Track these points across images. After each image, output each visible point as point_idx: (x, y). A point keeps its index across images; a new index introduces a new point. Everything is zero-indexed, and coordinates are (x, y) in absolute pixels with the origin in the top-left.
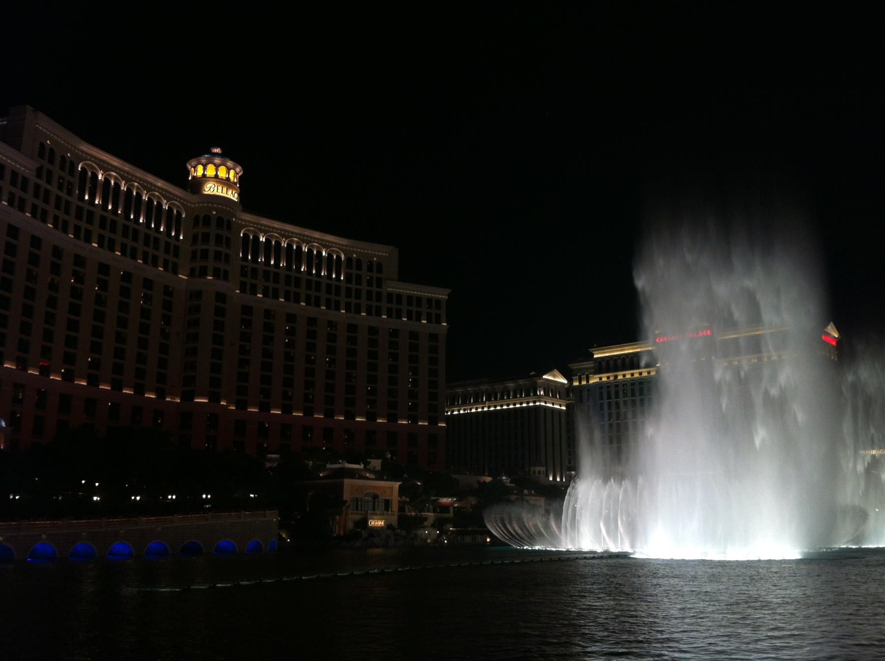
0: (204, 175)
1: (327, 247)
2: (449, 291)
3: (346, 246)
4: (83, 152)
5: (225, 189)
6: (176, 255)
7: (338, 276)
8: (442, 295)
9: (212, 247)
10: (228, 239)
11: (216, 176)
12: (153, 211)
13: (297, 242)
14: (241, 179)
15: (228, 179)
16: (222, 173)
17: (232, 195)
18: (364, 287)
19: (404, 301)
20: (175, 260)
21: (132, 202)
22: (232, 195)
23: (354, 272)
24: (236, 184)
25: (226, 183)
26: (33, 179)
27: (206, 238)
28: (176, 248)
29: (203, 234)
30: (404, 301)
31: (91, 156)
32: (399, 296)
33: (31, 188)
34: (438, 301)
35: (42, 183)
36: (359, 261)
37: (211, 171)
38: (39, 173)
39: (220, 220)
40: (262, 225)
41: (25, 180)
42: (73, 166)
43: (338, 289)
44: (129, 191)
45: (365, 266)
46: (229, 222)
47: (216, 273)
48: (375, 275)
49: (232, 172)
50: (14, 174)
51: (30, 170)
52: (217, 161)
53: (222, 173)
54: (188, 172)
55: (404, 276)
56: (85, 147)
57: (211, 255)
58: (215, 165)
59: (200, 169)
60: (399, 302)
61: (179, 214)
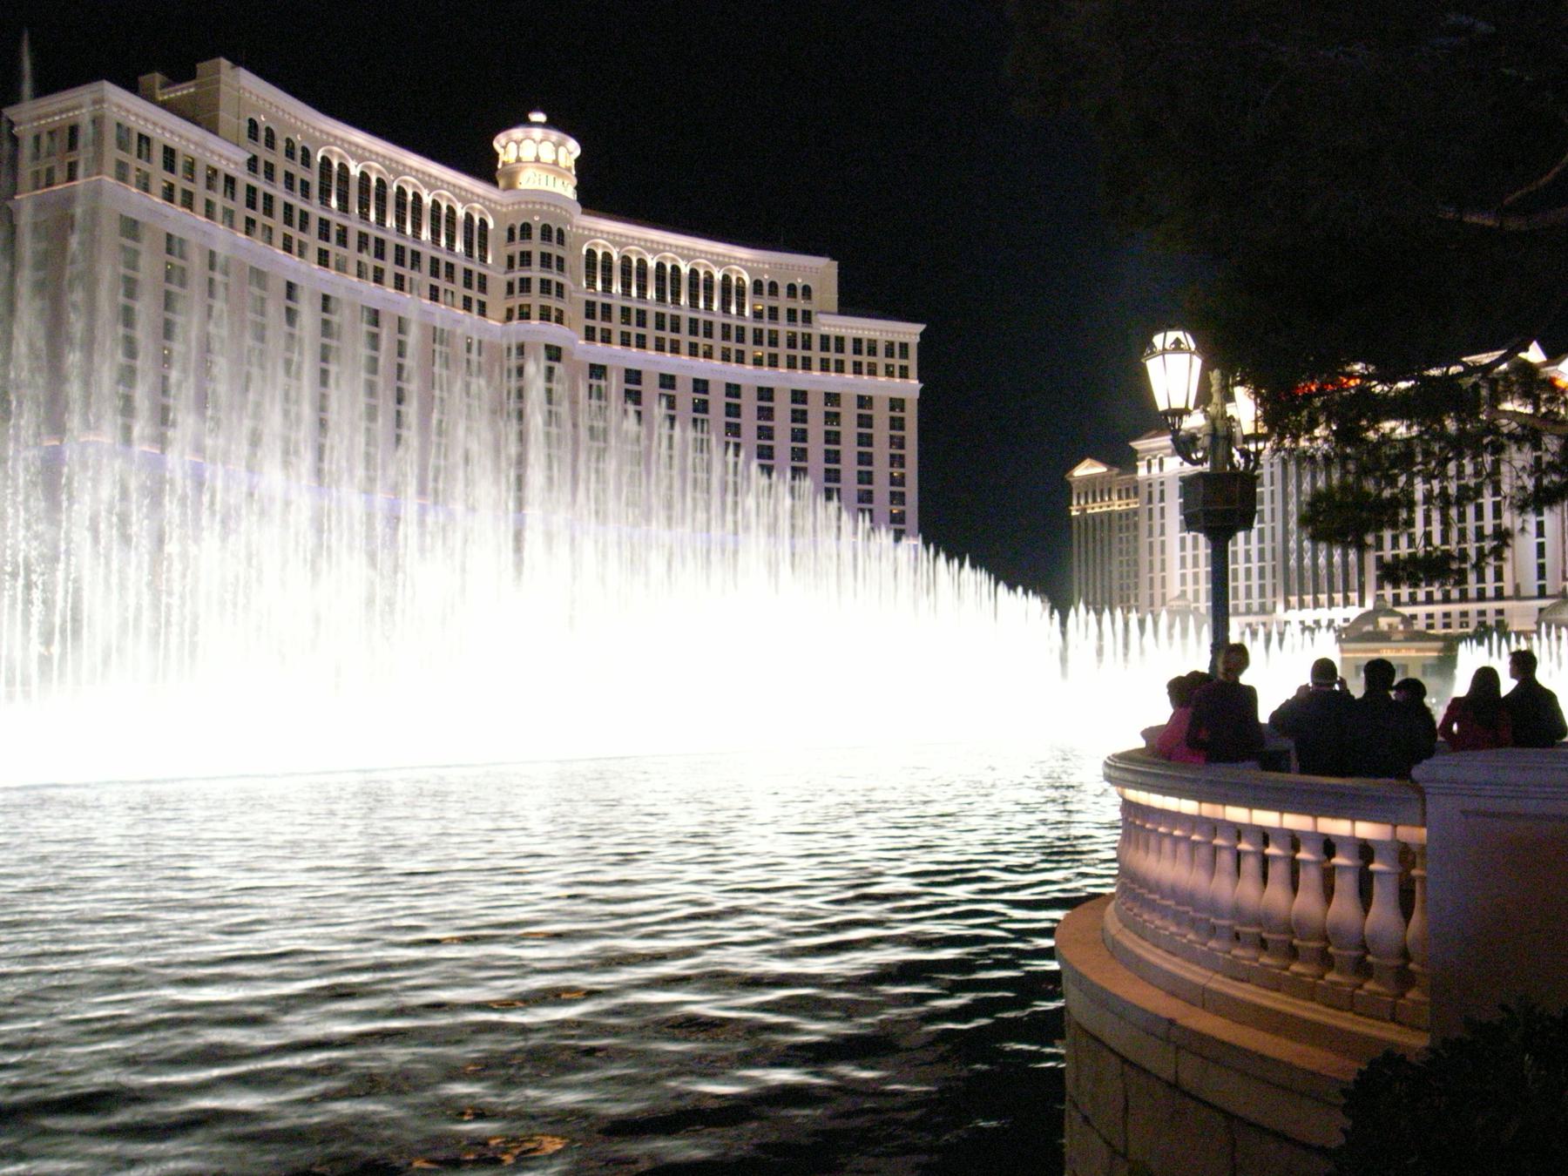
0: (519, 160)
2: (921, 327)
4: (321, 131)
5: (551, 177)
6: (483, 287)
7: (741, 312)
8: (910, 333)
9: (536, 273)
10: (560, 260)
11: (537, 160)
12: (442, 220)
14: (579, 162)
15: (556, 163)
16: (547, 153)
18: (783, 327)
19: (849, 346)
20: (482, 297)
21: (409, 207)
22: (567, 188)
23: (764, 303)
24: (569, 169)
27: (526, 258)
28: (483, 278)
29: (522, 254)
30: (849, 346)
31: (336, 137)
32: (840, 341)
34: (904, 347)
36: (773, 287)
37: (528, 151)
38: (252, 164)
39: (546, 232)
41: (230, 181)
43: (741, 332)
45: (783, 291)
46: (561, 232)
47: (545, 315)
49: (562, 150)
50: (213, 173)
51: (236, 164)
52: (537, 133)
54: (496, 155)
55: (850, 303)
57: (536, 286)
59: (512, 146)
60: (840, 348)
61: (483, 223)
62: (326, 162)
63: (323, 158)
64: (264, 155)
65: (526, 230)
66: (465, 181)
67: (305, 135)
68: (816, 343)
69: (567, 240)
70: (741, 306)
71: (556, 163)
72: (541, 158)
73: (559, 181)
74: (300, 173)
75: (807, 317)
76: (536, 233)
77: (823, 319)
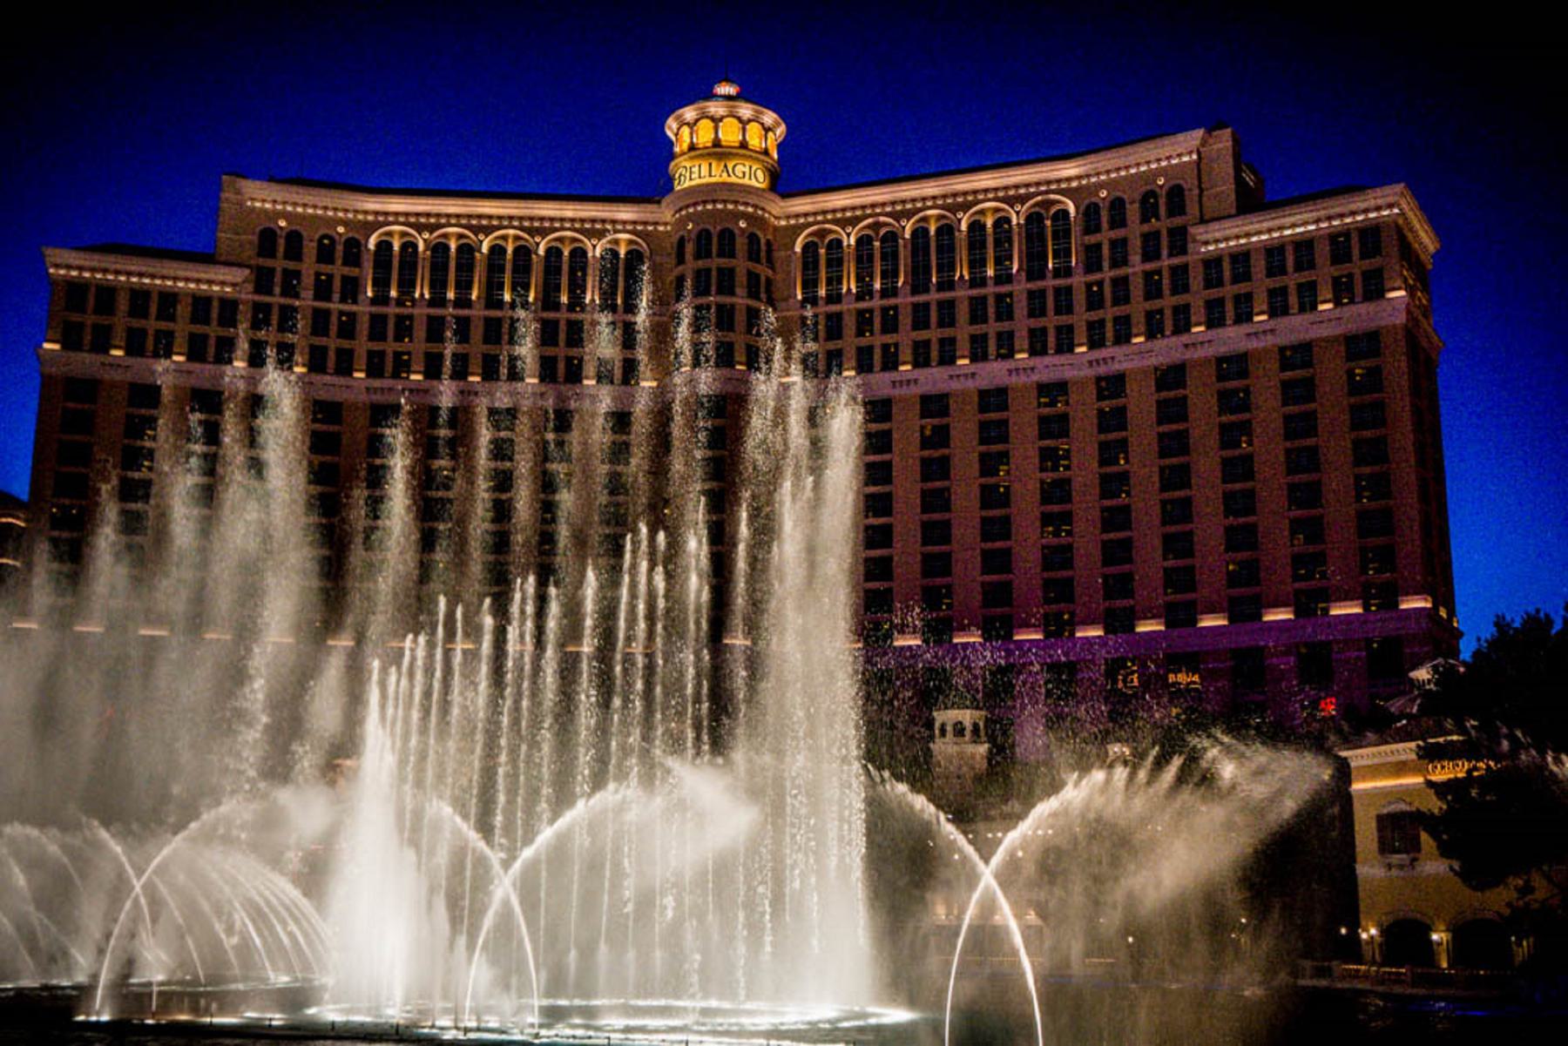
3: (1079, 177)
15: (717, 143)
16: (705, 135)
19: (1259, 266)
25: (718, 151)
26: (247, 295)
32: (1241, 259)
36: (1117, 205)
38: (262, 281)
41: (229, 308)
42: (353, 250)
45: (1133, 211)
48: (1162, 224)
51: (234, 285)
56: (373, 204)
58: (713, 119)
62: (384, 246)
63: (379, 245)
64: (279, 264)
65: (682, 242)
67: (345, 223)
68: (1196, 280)
69: (741, 243)
70: (1063, 253)
71: (717, 143)
72: (722, 142)
73: (717, 168)
75: (1180, 240)
76: (690, 248)
77: (1198, 232)
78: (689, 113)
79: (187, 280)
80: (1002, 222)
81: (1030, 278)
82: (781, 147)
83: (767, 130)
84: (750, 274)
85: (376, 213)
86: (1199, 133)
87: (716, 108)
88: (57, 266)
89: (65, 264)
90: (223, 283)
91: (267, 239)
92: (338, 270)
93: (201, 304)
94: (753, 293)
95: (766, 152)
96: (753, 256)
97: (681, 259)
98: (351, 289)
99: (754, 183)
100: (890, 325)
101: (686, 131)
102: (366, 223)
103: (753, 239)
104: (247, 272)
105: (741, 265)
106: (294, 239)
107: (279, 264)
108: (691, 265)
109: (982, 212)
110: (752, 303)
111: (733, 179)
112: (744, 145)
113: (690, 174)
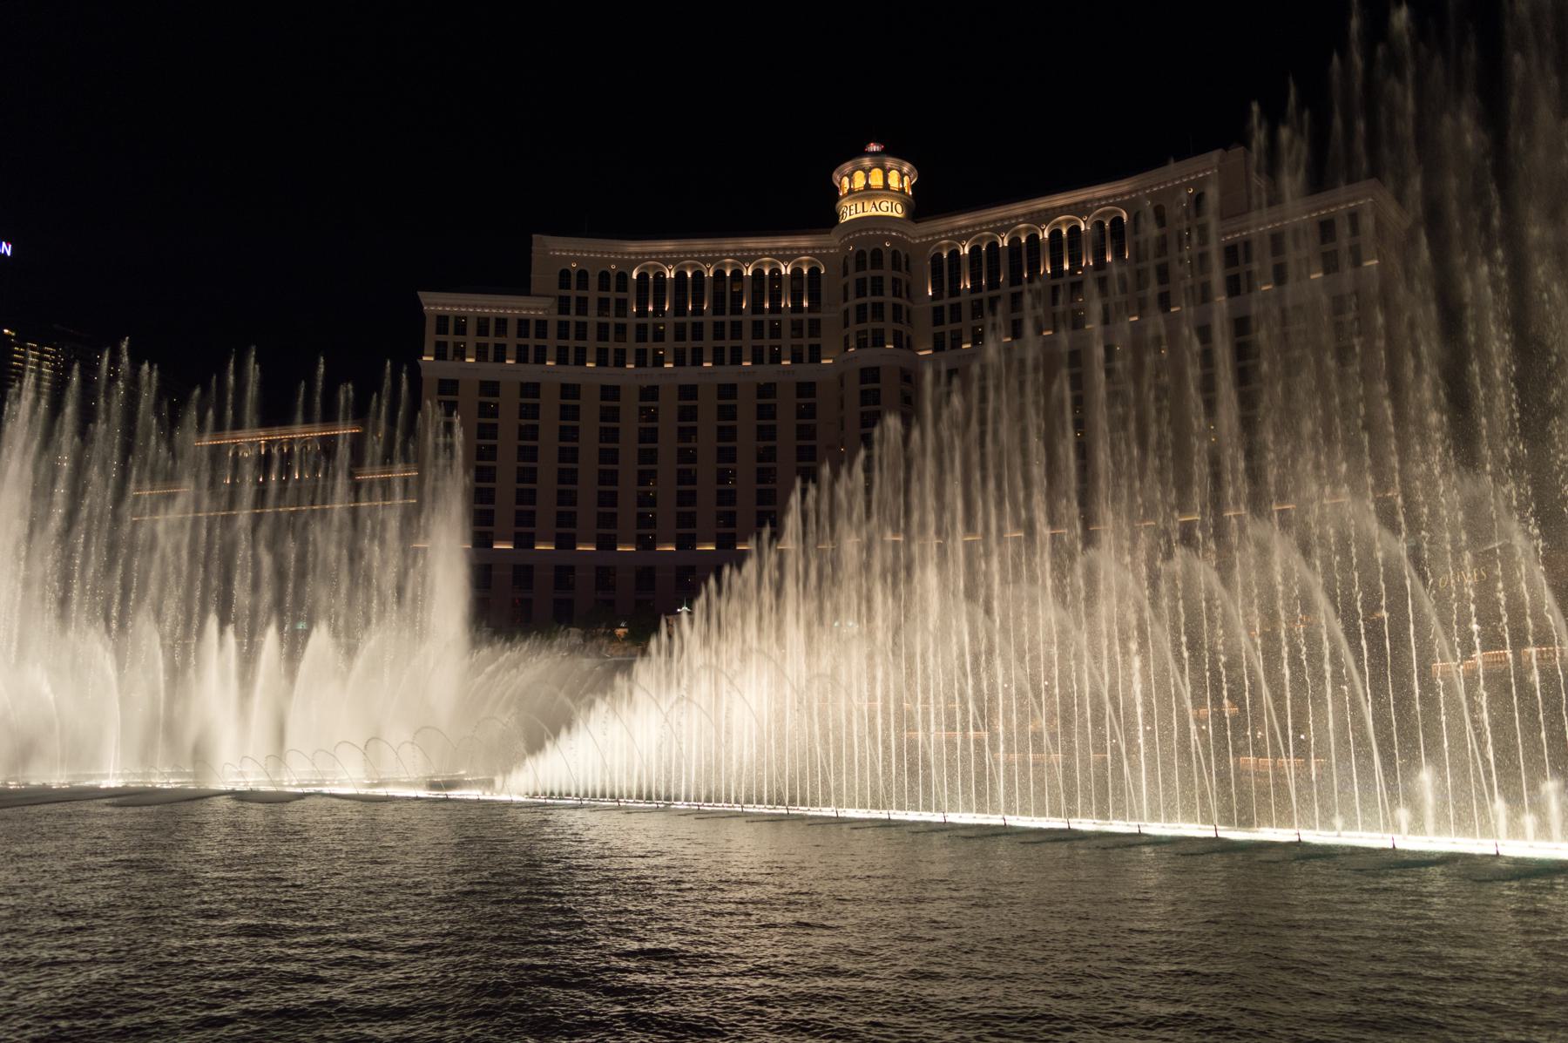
1: (786, 259)
3: (1129, 193)
13: (1028, 229)
15: (867, 187)
16: (859, 181)
17: (891, 209)
25: (868, 192)
26: (554, 317)
33: (552, 330)
35: (572, 318)
40: (960, 228)
41: (542, 325)
42: (623, 277)
44: (719, 274)
53: (876, 179)
56: (634, 247)
64: (573, 293)
66: (804, 241)
69: (887, 259)
74: (613, 295)
78: (848, 167)
79: (513, 308)
80: (1074, 231)
81: (676, 315)
82: (913, 187)
83: (902, 175)
84: (895, 281)
85: (637, 254)
86: (1215, 156)
87: (867, 162)
88: (429, 304)
89: (435, 304)
90: (537, 309)
91: (565, 274)
92: (613, 295)
93: (523, 324)
94: (896, 294)
95: (902, 190)
96: (896, 265)
97: (846, 273)
98: (622, 306)
99: (895, 214)
100: (776, 332)
101: (846, 180)
102: (630, 261)
103: (895, 254)
104: (551, 300)
105: (887, 273)
106: (583, 275)
107: (573, 293)
108: (853, 276)
109: (1058, 223)
110: (897, 300)
111: (880, 213)
112: (886, 186)
113: (851, 211)
